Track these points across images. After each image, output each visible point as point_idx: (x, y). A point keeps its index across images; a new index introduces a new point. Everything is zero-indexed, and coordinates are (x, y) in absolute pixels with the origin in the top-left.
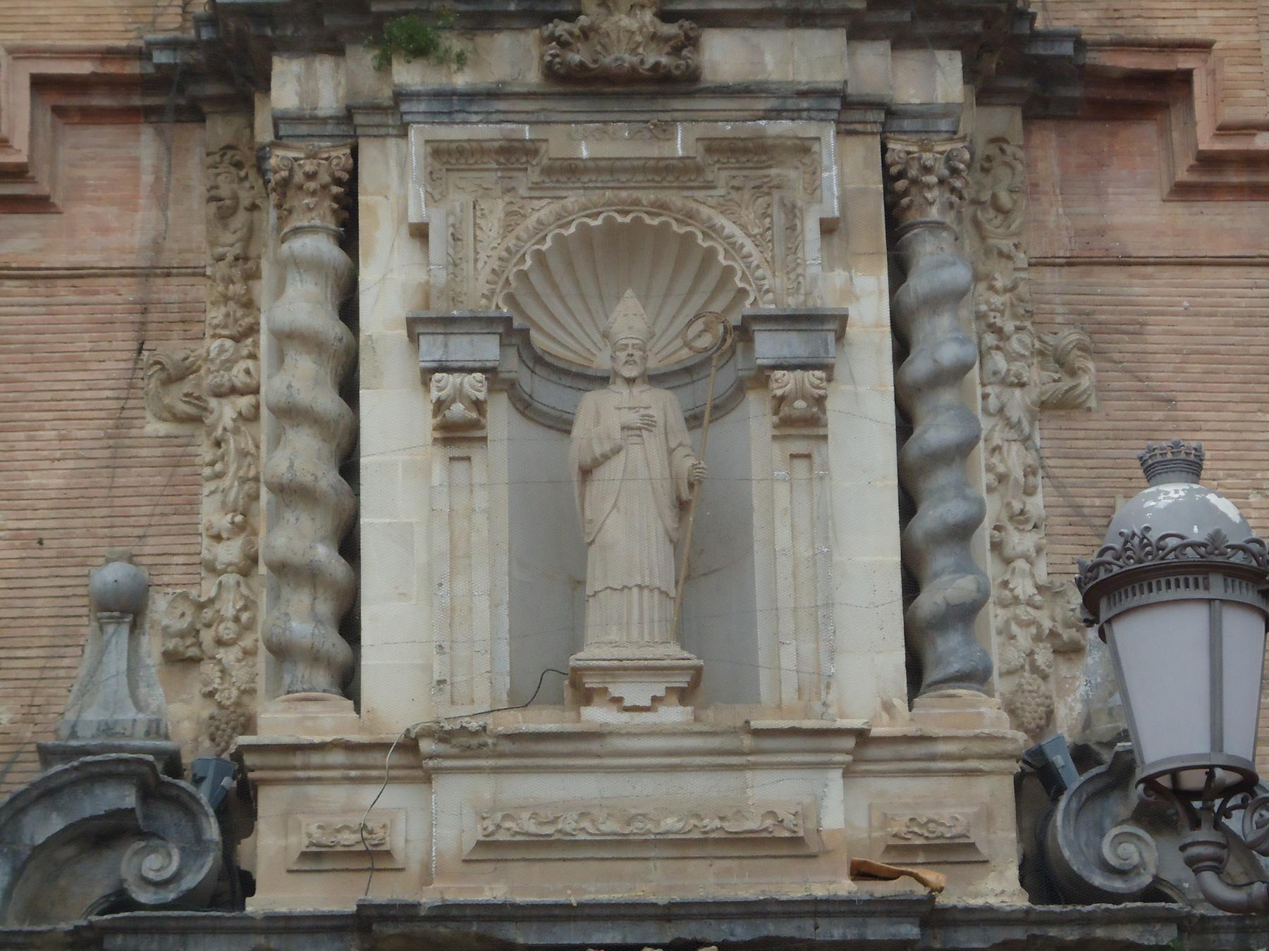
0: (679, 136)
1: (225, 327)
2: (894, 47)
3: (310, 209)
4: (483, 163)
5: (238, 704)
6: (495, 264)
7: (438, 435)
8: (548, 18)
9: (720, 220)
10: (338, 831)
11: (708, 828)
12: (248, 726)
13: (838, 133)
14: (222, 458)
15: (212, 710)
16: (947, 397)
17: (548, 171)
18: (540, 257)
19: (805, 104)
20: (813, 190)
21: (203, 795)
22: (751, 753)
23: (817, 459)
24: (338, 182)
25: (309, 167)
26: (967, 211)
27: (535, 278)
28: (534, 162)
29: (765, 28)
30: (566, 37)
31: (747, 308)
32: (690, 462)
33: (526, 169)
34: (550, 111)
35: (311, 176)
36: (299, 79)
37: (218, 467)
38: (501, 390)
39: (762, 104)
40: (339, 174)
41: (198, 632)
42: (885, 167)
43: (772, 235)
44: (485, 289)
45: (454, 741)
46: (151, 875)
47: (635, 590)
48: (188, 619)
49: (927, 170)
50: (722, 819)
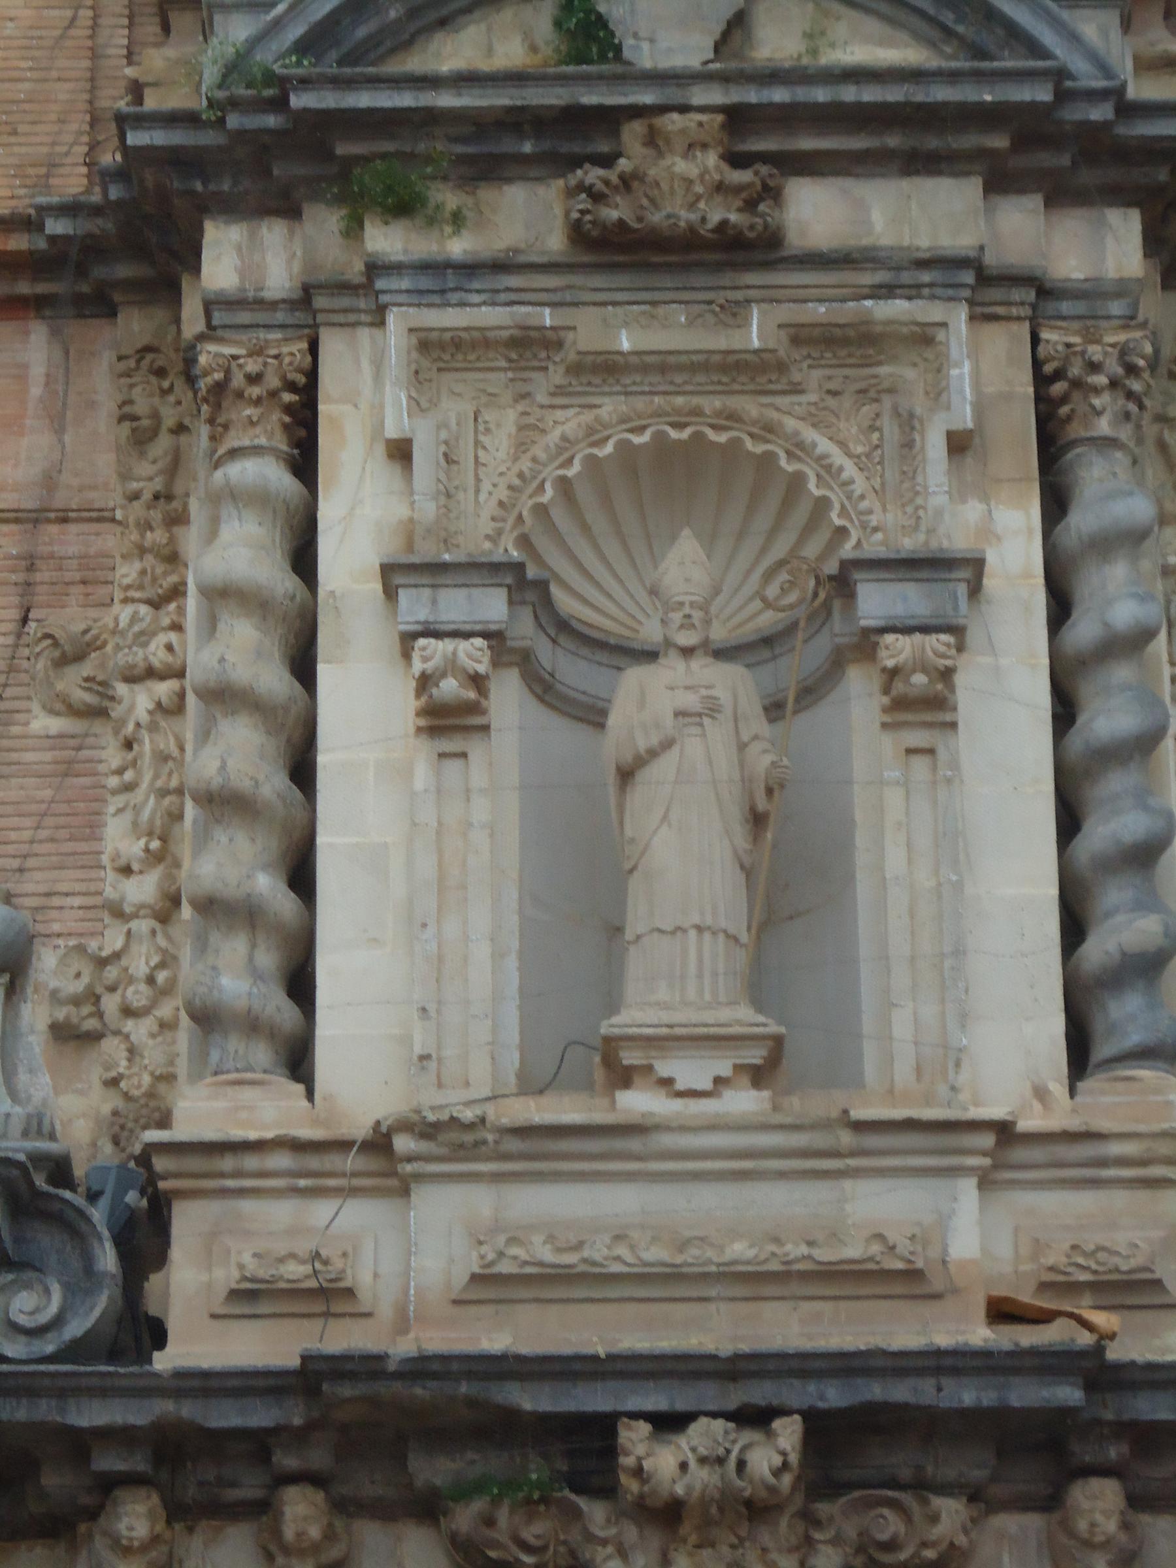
0: (755, 322)
1: (141, 587)
2: (1047, 205)
3: (252, 424)
4: (488, 360)
5: (151, 1095)
6: (503, 494)
7: (422, 722)
8: (576, 162)
9: (810, 434)
10: (281, 1260)
11: (791, 1257)
12: (164, 1122)
13: (972, 318)
14: (134, 763)
15: (117, 1102)
16: (1122, 673)
17: (575, 369)
18: (565, 486)
19: (926, 277)
20: (938, 394)
21: (98, 1214)
22: (853, 1154)
23: (942, 754)
24: (291, 387)
25: (252, 366)
26: (1151, 430)
27: (559, 516)
28: (557, 359)
29: (872, 175)
30: (600, 186)
31: (847, 550)
32: (767, 759)
33: (546, 368)
34: (581, 288)
35: (254, 379)
36: (239, 249)
37: (129, 776)
38: (510, 664)
39: (868, 278)
40: (291, 376)
41: (97, 999)
42: (1037, 364)
43: (882, 456)
44: (488, 528)
45: (440, 1138)
46: (23, 1320)
47: (693, 933)
48: (85, 980)
49: (1094, 367)
50: (810, 1244)
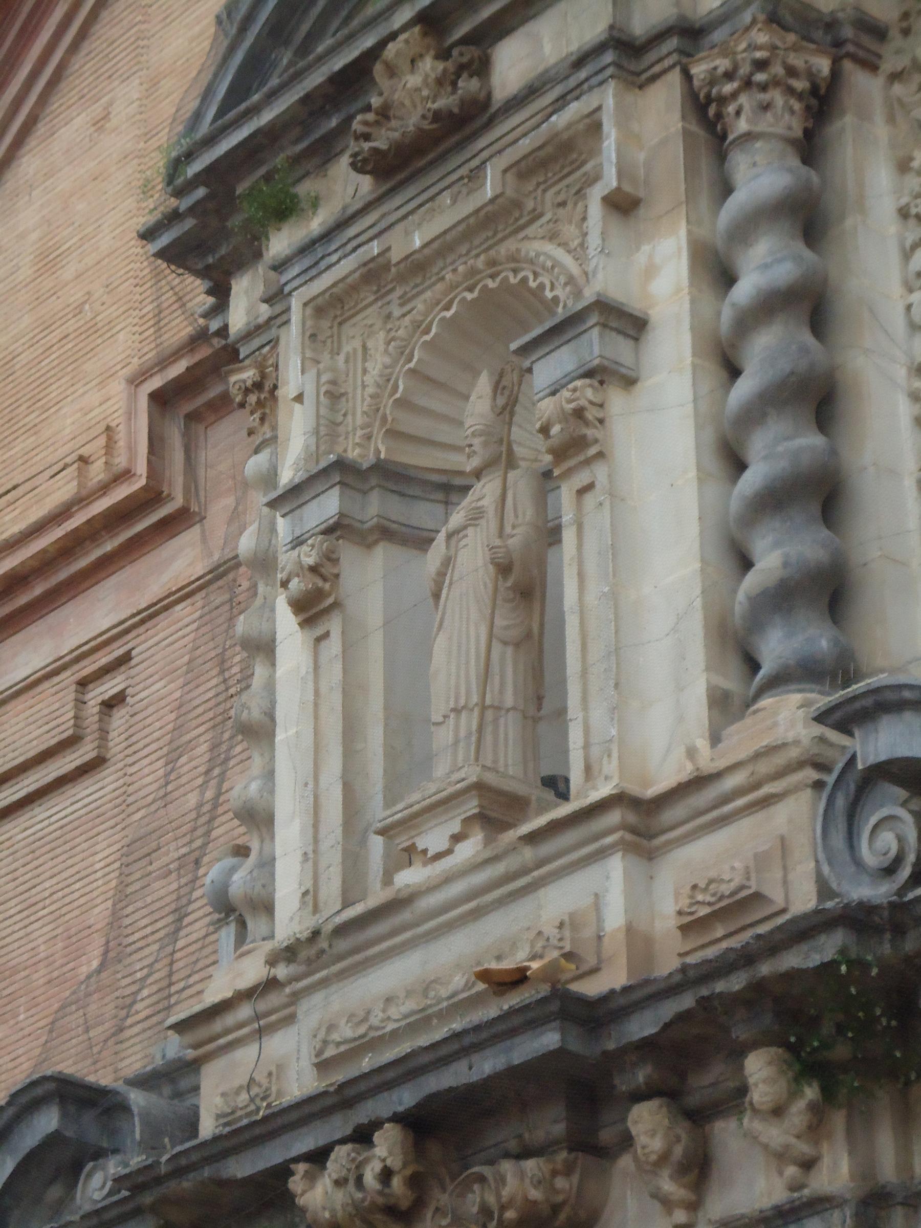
4: (362, 300)
19: (583, 74)
22: (540, 864)
38: (376, 542)
